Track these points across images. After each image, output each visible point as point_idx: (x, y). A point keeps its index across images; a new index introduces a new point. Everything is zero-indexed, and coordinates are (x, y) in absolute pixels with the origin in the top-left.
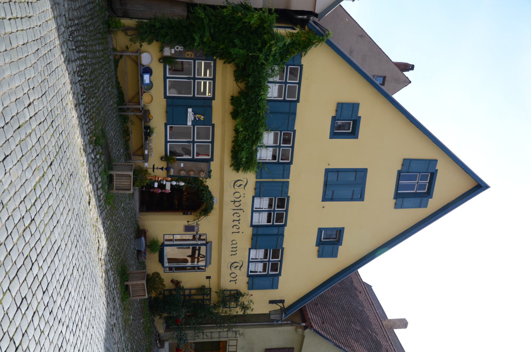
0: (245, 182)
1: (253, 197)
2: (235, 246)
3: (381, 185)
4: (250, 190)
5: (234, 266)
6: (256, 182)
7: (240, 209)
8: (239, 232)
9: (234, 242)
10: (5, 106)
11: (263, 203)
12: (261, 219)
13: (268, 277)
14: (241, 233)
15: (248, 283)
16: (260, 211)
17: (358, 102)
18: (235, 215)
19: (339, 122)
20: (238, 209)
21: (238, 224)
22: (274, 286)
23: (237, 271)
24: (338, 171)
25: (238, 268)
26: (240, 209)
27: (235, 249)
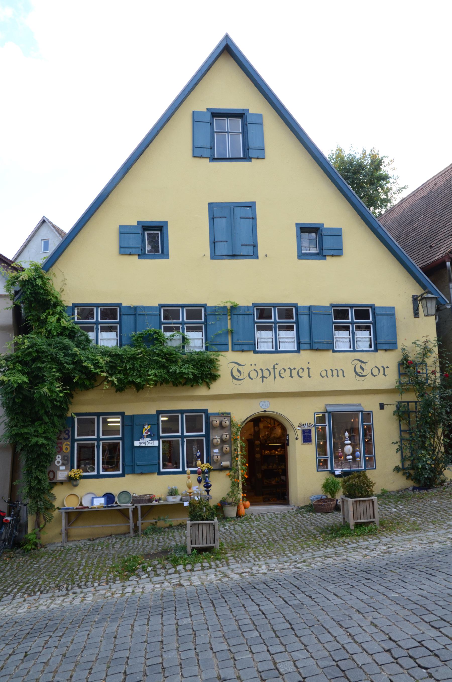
1: (256, 352)
3: (231, 182)
4: (246, 358)
5: (361, 371)
6: (233, 350)
7: (274, 368)
8: (308, 369)
9: (324, 374)
11: (264, 338)
16: (276, 342)
18: (282, 375)
20: (274, 372)
21: (296, 370)
22: (390, 313)
23: (368, 368)
24: (213, 243)
25: (363, 365)
26: (274, 368)
27: (335, 373)
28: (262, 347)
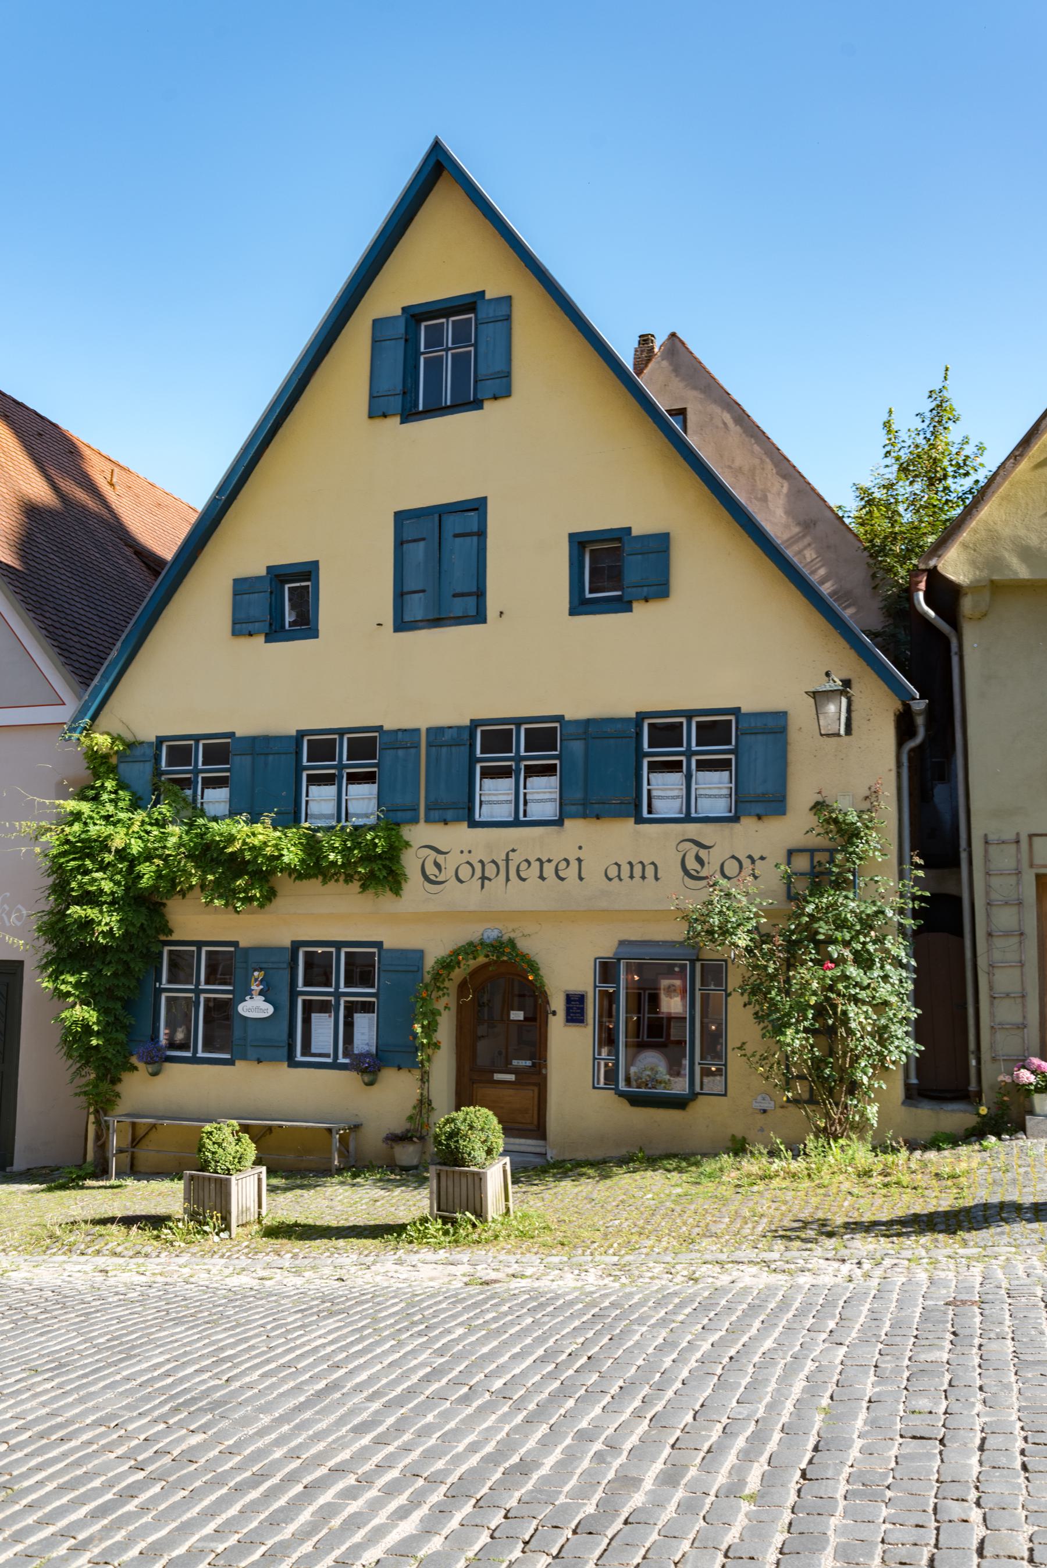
0: (428, 851)
1: (473, 824)
2: (625, 869)
3: (438, 458)
4: (455, 837)
5: (698, 867)
6: (428, 820)
7: (507, 860)
8: (579, 860)
9: (613, 872)
10: (1026, 1555)
11: (495, 796)
12: (543, 795)
13: (740, 747)
14: (581, 854)
15: (759, 817)
16: (519, 801)
17: (231, 582)
18: (523, 875)
19: (289, 617)
20: (507, 867)
21: (554, 864)
22: (773, 727)
23: (714, 859)
24: (400, 595)
25: (703, 854)
26: (507, 860)
27: (638, 869)
28: (482, 813)
